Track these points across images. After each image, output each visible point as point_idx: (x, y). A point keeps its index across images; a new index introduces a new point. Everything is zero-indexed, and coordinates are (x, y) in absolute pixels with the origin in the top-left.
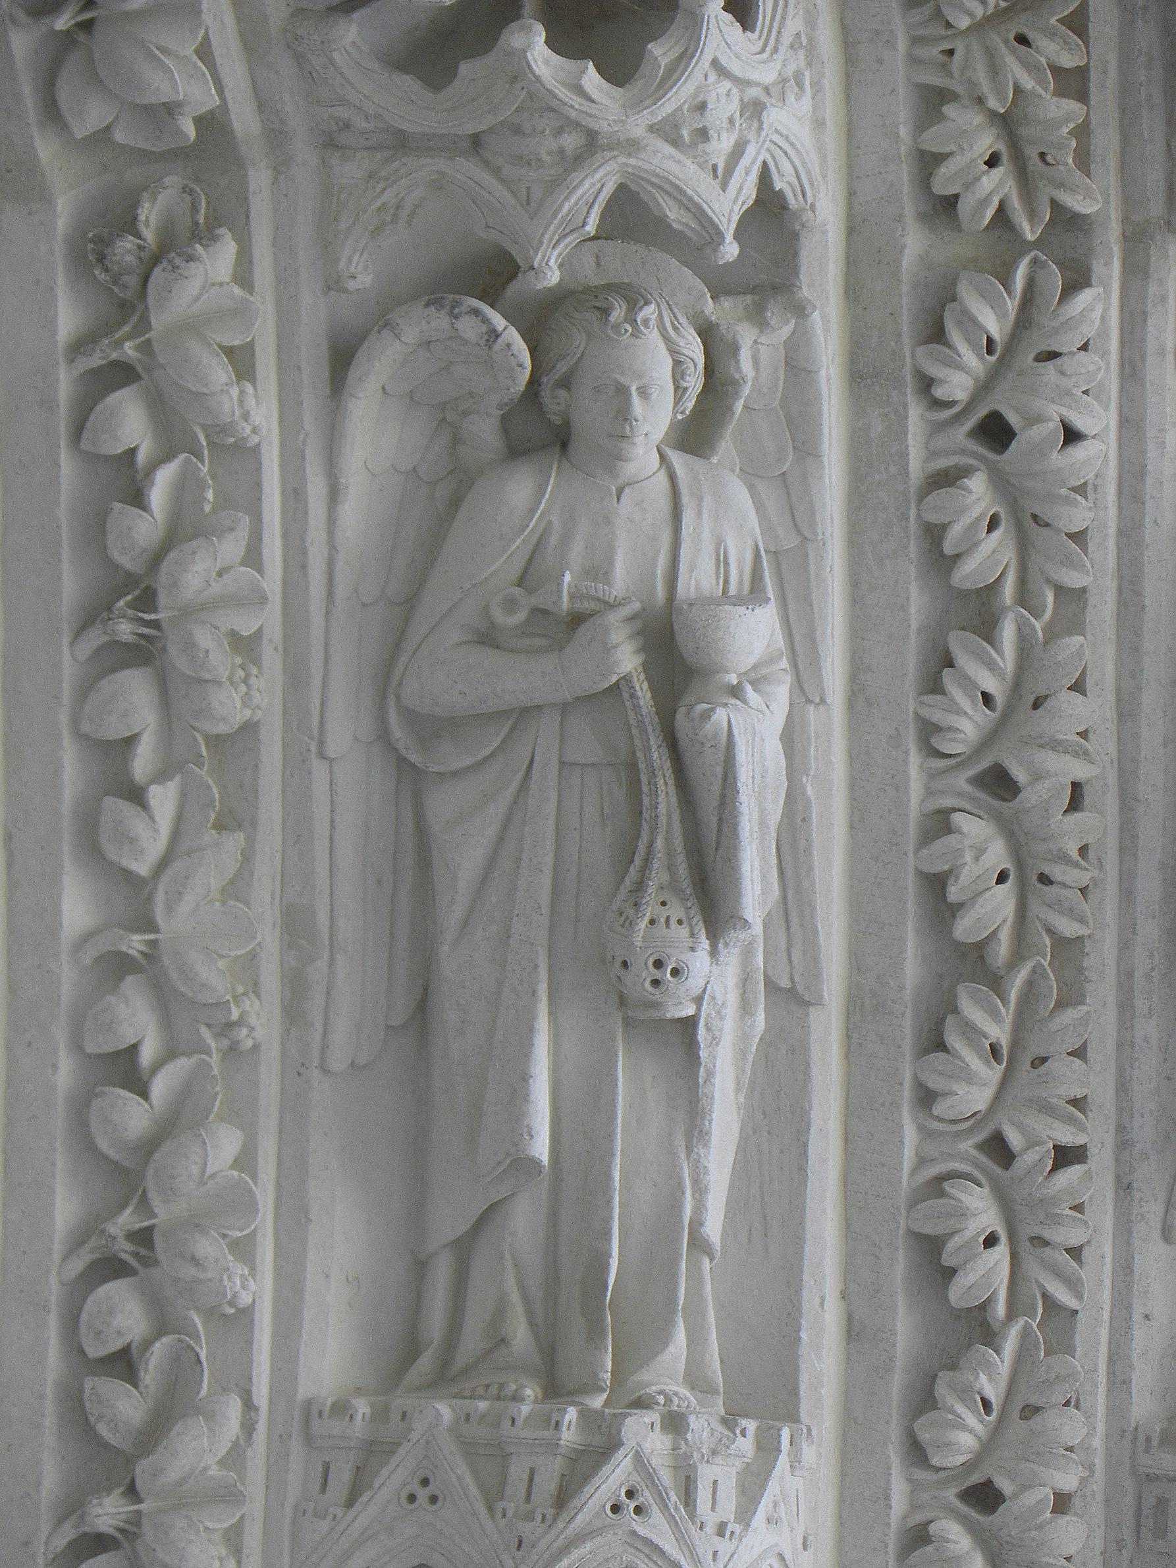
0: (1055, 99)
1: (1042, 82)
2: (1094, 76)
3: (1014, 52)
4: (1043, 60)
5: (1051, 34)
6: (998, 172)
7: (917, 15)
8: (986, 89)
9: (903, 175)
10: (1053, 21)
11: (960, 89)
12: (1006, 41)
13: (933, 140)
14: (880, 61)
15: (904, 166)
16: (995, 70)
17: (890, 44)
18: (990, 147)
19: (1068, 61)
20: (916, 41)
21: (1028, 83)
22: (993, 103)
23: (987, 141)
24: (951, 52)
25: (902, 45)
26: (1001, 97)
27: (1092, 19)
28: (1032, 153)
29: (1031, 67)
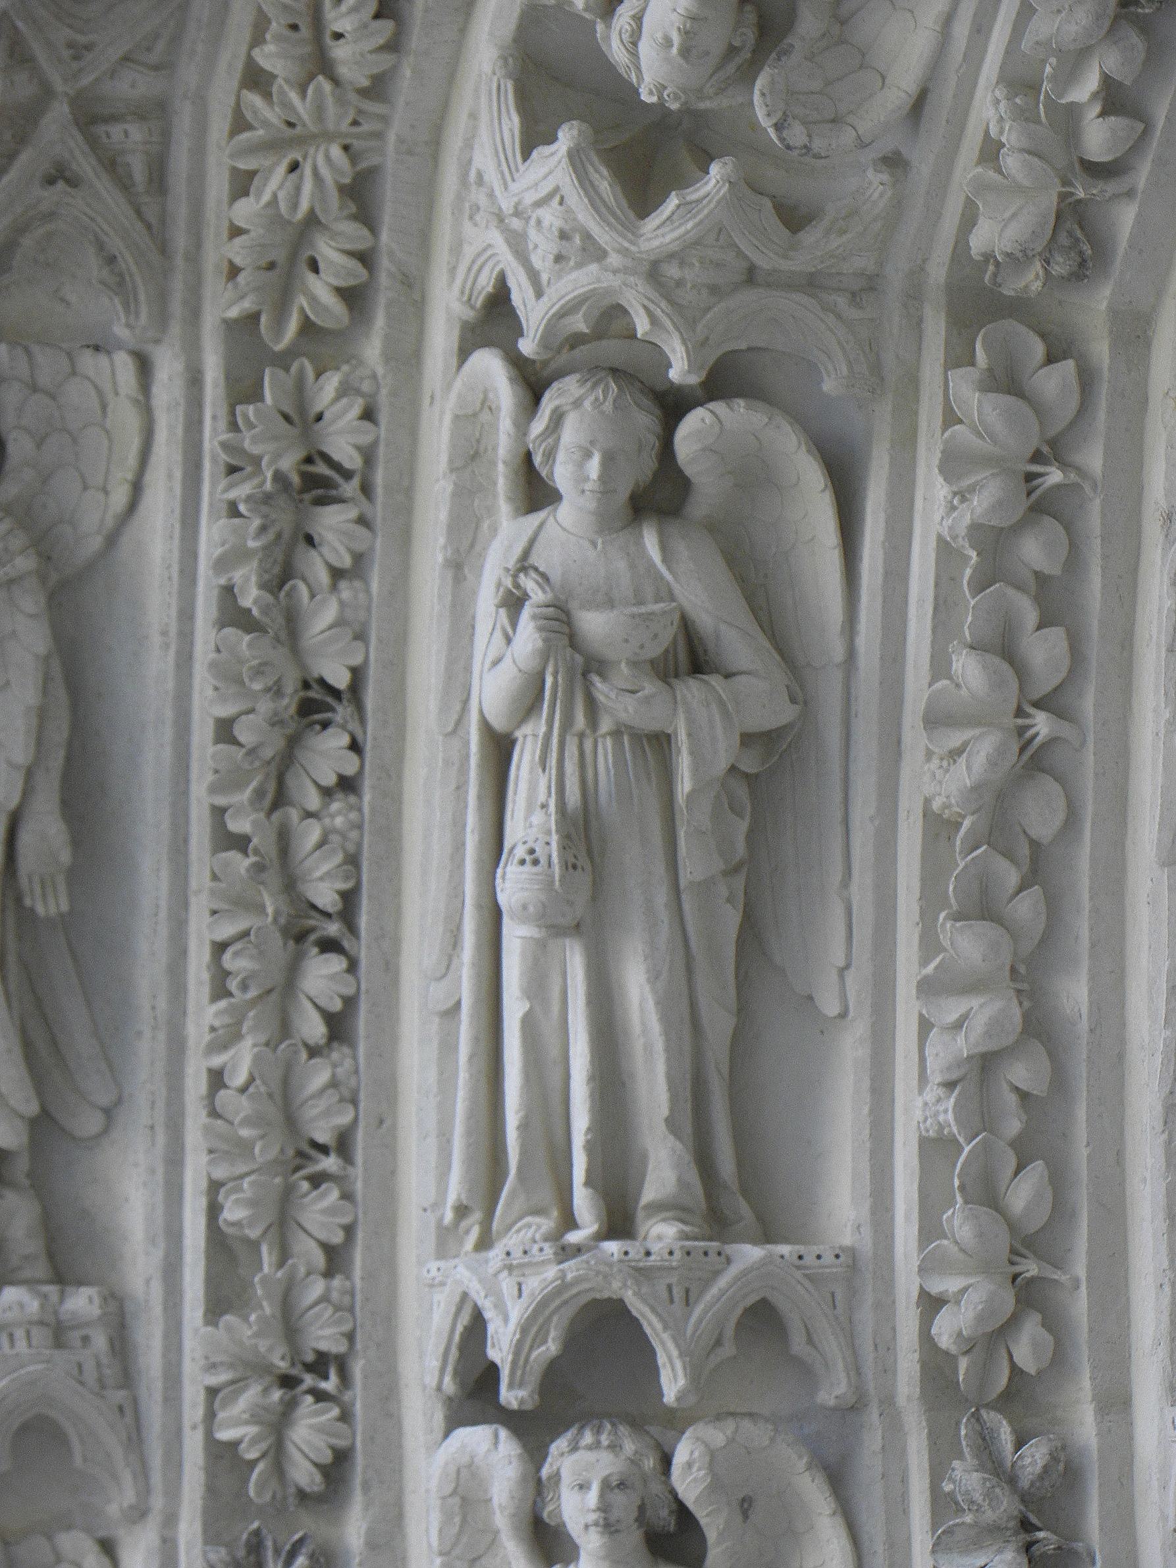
0: (276, 72)
1: (282, 93)
2: (235, 84)
3: (300, 118)
4: (277, 109)
5: (266, 123)
6: (338, 27)
7: (374, 160)
8: (330, 101)
9: (416, 39)
10: (261, 132)
11: (352, 97)
12: (304, 125)
13: (385, 61)
14: (413, 127)
15: (413, 46)
16: (319, 111)
17: (401, 140)
18: (337, 46)
19: (253, 99)
20: (379, 135)
21: (294, 96)
22: (327, 87)
23: (341, 52)
24: (355, 123)
25: (391, 137)
26: (319, 91)
27: (230, 111)
28: (305, 32)
29: (287, 105)
